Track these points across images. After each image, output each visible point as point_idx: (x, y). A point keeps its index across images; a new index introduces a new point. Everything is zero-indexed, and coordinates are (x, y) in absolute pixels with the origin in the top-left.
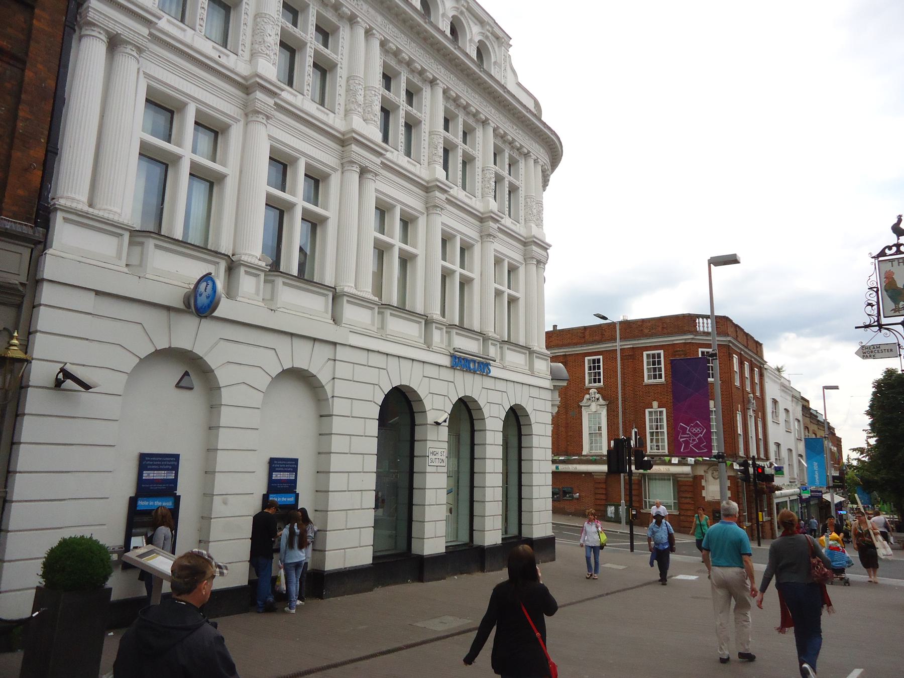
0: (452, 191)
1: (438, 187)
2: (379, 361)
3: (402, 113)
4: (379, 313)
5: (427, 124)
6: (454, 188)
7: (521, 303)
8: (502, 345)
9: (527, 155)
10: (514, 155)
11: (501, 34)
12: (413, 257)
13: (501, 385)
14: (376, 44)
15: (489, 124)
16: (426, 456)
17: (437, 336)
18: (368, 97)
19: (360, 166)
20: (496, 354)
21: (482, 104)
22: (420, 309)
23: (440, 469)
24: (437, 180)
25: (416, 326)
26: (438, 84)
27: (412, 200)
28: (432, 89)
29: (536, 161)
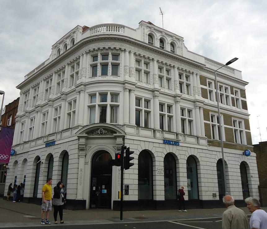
2: (138, 143)
10: (188, 74)
11: (179, 38)
13: (184, 149)
14: (132, 55)
17: (158, 135)
19: (129, 89)
23: (161, 175)
24: (155, 88)
29: (196, 74)
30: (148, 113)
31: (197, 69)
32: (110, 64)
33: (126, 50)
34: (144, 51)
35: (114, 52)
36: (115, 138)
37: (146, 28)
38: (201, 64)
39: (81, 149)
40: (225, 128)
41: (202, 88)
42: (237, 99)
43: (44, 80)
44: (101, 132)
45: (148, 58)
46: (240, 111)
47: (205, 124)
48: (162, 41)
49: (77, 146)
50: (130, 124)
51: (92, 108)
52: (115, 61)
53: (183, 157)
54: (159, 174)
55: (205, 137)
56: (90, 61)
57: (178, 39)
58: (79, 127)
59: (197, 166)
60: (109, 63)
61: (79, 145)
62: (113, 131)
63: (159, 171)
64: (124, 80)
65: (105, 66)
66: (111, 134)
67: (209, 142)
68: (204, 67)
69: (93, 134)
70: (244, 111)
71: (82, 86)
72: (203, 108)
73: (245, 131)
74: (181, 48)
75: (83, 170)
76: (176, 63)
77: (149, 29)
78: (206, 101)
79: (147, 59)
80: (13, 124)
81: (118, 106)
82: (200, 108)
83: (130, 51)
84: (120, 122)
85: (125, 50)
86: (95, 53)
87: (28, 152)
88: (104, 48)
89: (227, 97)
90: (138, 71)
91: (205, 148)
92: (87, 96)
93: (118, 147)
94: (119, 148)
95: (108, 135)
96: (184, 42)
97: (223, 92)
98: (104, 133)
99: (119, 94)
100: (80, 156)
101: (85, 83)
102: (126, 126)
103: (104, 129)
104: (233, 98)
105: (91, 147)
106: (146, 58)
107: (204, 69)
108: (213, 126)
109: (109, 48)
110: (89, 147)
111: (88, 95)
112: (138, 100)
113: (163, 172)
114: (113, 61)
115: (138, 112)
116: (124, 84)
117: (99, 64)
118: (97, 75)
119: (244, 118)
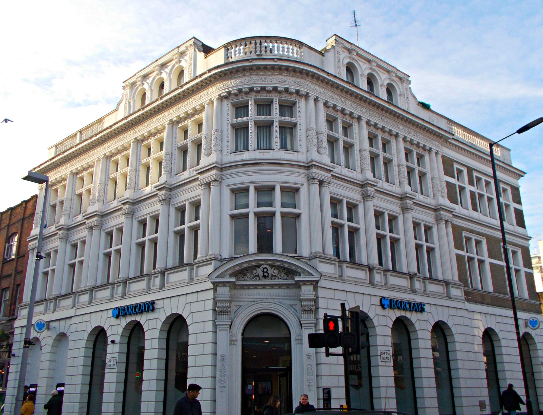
0: (378, 185)
1: (369, 183)
3: (341, 143)
4: (339, 266)
5: (358, 145)
6: (379, 182)
7: (437, 251)
8: (424, 281)
9: (430, 150)
10: (420, 152)
11: (401, 75)
12: (357, 230)
15: (399, 136)
16: (378, 355)
18: (319, 137)
20: (421, 286)
21: (392, 125)
22: (365, 262)
23: (388, 364)
25: (363, 272)
26: (362, 119)
27: (354, 195)
28: (359, 123)
29: (437, 153)
30: (353, 232)
31: (437, 143)
32: (276, 124)
33: (310, 94)
34: (343, 100)
35: (285, 97)
36: (298, 285)
37: (342, 51)
39: (221, 312)
40: (491, 264)
41: (447, 183)
44: (264, 272)
45: (351, 114)
46: (513, 230)
47: (458, 256)
48: (371, 81)
49: (210, 305)
50: (325, 256)
52: (287, 119)
53: (424, 325)
54: (384, 364)
55: (459, 283)
56: (230, 116)
57: (400, 79)
58: (213, 262)
60: (275, 123)
61: (215, 302)
62: (290, 272)
63: (384, 356)
64: (309, 160)
66: (285, 277)
67: (466, 293)
68: (450, 138)
69: (246, 278)
70: (520, 230)
71: (214, 172)
72: (452, 222)
73: (523, 270)
74: (406, 98)
76: (401, 127)
77: (346, 54)
78: (457, 208)
79: (347, 116)
80: (22, 255)
81: (298, 216)
82: (446, 221)
83: (317, 97)
84: (305, 251)
85: (307, 96)
86: (241, 99)
88: (263, 89)
90: (332, 142)
91: (461, 305)
92: (227, 193)
93: (306, 306)
94: (306, 308)
95: (279, 278)
96: (410, 86)
98: (272, 275)
99: (297, 190)
100: (218, 326)
101: (222, 165)
102: (318, 260)
103: (272, 266)
105: (241, 306)
106: (345, 114)
107: (450, 143)
108: (471, 259)
109: (275, 89)
110: (235, 306)
111: (229, 191)
112: (335, 202)
113: (392, 357)
114: (283, 117)
115: (337, 229)
116: (308, 168)
117: (251, 125)
118: (250, 147)
119: (520, 245)
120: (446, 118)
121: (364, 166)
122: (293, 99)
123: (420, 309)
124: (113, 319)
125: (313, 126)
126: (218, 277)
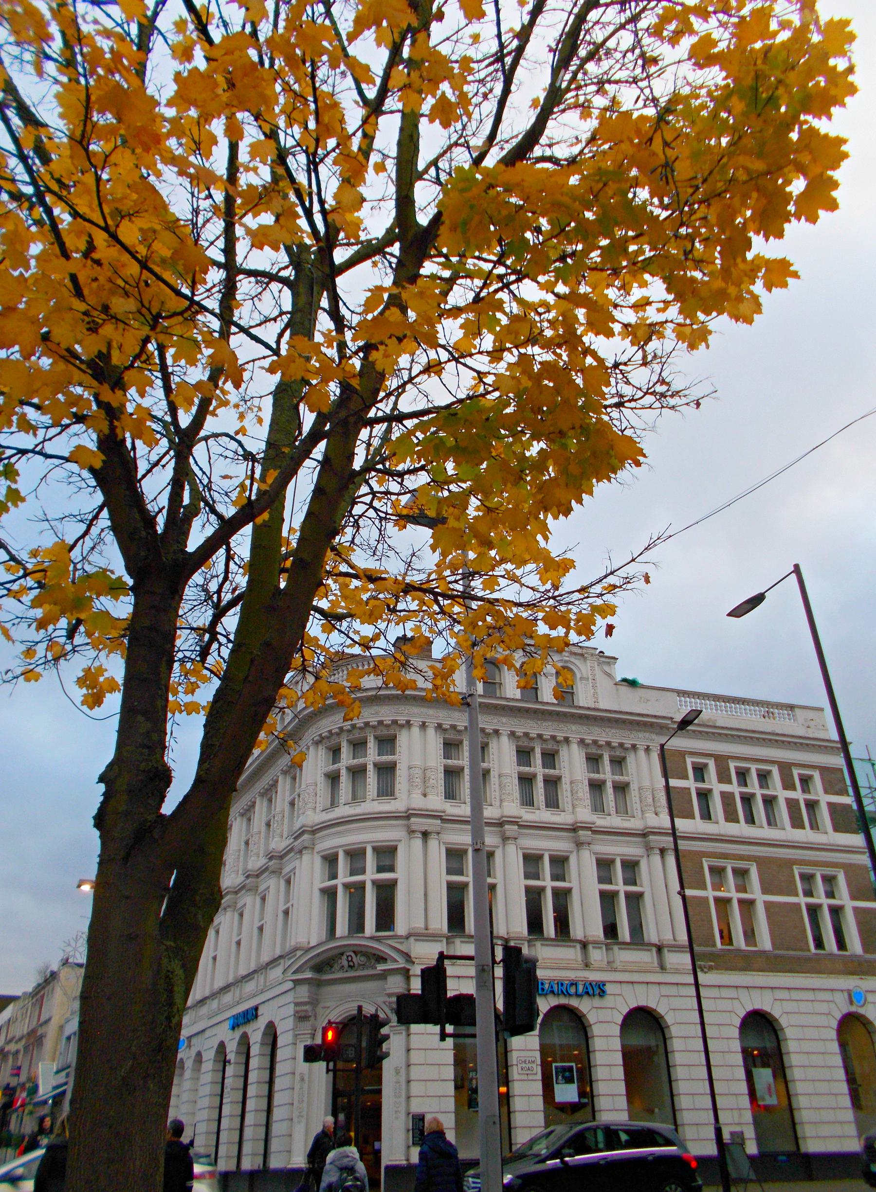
10: (618, 753)
14: (431, 732)
31: (647, 735)
38: (655, 717)
42: (812, 805)
43: (242, 815)
51: (330, 894)
54: (525, 1077)
57: (582, 655)
59: (665, 1040)
65: (357, 772)
71: (306, 836)
75: (306, 1078)
86: (334, 741)
87: (203, 1031)
89: (769, 802)
92: (318, 861)
97: (754, 787)
104: (792, 805)
109: (367, 724)
113: (539, 1068)
120: (672, 690)
121: (503, 797)
122: (392, 732)
123: (597, 991)
124: (231, 1032)
125: (417, 762)
126: (294, 972)
